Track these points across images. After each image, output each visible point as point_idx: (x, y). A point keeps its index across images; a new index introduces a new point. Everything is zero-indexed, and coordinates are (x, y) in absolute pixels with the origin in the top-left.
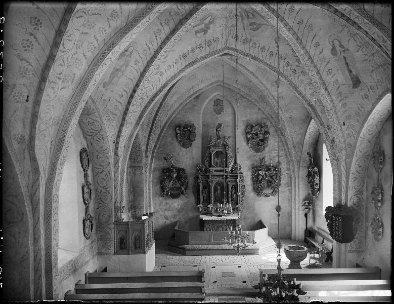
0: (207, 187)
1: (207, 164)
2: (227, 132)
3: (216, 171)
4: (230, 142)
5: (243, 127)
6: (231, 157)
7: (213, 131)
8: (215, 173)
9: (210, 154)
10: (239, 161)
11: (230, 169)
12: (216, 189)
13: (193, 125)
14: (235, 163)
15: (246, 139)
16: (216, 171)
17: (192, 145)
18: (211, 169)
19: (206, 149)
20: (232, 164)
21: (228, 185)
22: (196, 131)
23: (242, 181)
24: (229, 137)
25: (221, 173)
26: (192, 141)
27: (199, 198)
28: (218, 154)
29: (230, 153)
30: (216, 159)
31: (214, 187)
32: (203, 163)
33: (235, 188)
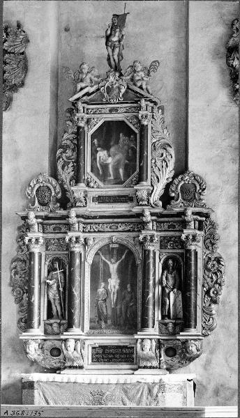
0: (64, 264)
1: (66, 174)
2: (151, 43)
3: (101, 199)
4: (162, 86)
5: (220, 30)
6: (165, 147)
7: (96, 50)
8: (94, 208)
9: (79, 133)
10: (194, 165)
11: (159, 190)
12: (98, 274)
13: (19, 26)
14: (182, 168)
15: (228, 77)
16: (101, 199)
17: (14, 104)
18: (78, 191)
19: (64, 111)
20: (167, 175)
21: (146, 254)
22: (31, 51)
23: (211, 241)
24: (155, 65)
25: (121, 208)
26: (14, 88)
27: (30, 304)
28: (109, 134)
29: (159, 131)
30: (102, 154)
31: (94, 267)
32: (54, 174)
33: (180, 267)
